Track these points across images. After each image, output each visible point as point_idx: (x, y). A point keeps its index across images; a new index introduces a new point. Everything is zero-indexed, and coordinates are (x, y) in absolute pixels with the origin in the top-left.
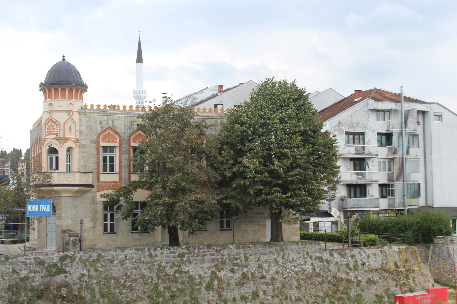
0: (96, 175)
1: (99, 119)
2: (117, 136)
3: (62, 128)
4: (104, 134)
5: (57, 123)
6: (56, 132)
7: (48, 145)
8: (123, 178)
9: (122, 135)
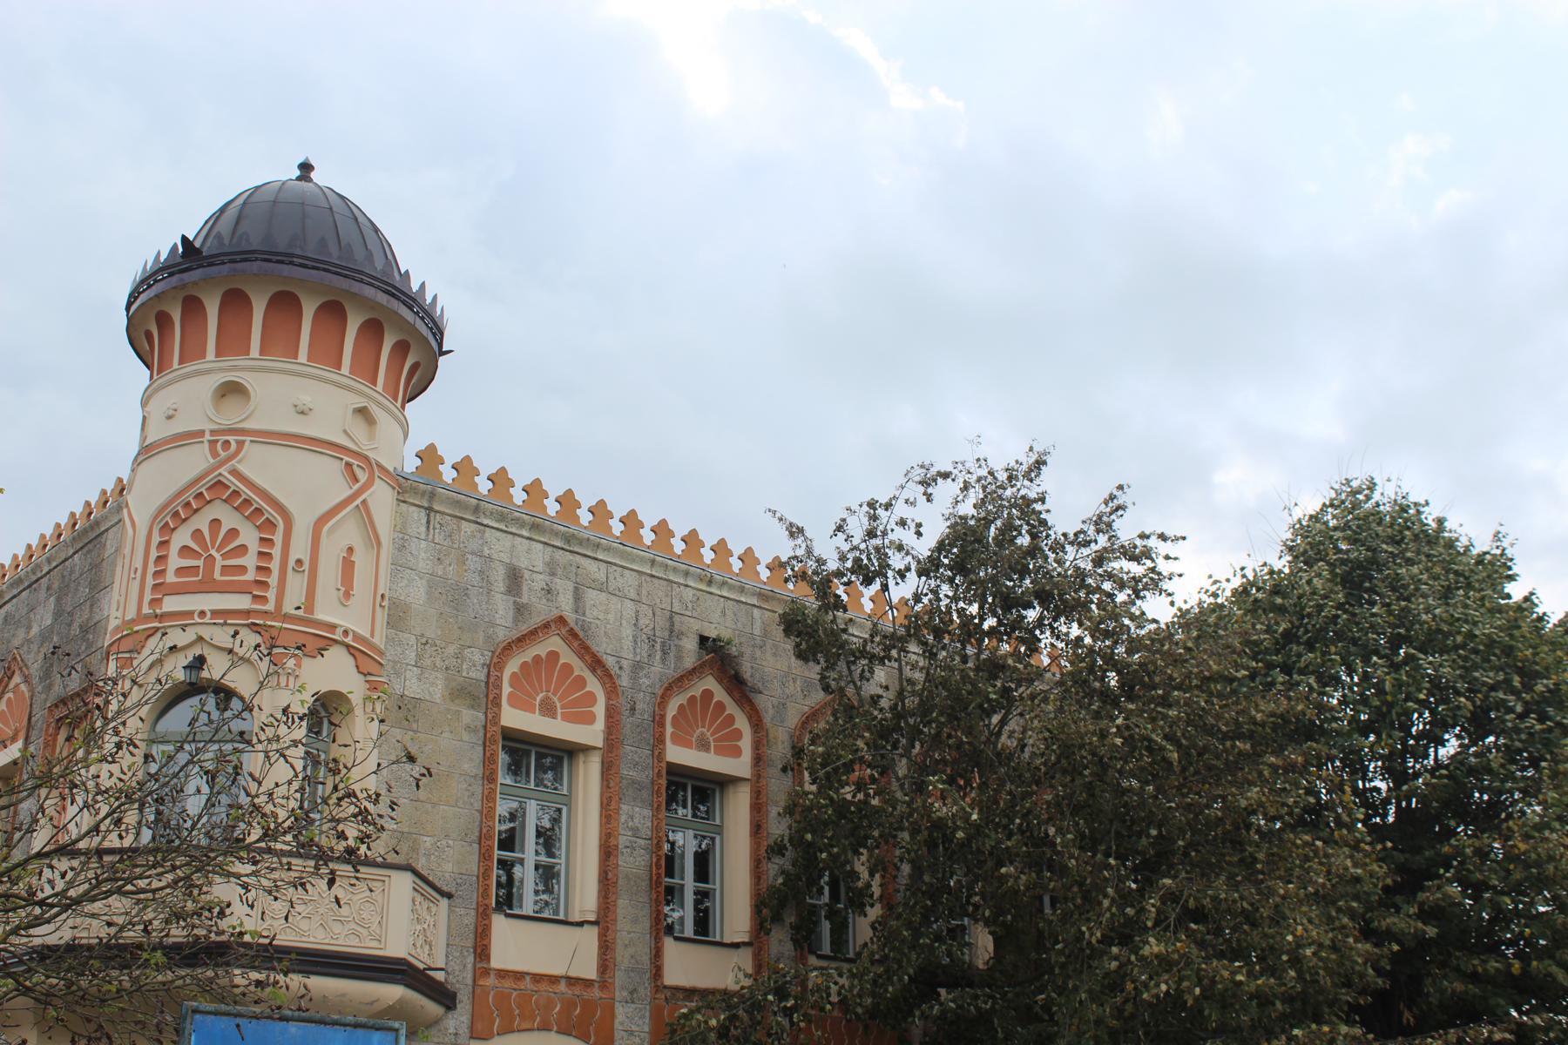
0: (470, 919)
2: (594, 685)
3: (300, 548)
4: (528, 655)
5: (265, 514)
6: (251, 575)
8: (622, 956)
9: (624, 681)
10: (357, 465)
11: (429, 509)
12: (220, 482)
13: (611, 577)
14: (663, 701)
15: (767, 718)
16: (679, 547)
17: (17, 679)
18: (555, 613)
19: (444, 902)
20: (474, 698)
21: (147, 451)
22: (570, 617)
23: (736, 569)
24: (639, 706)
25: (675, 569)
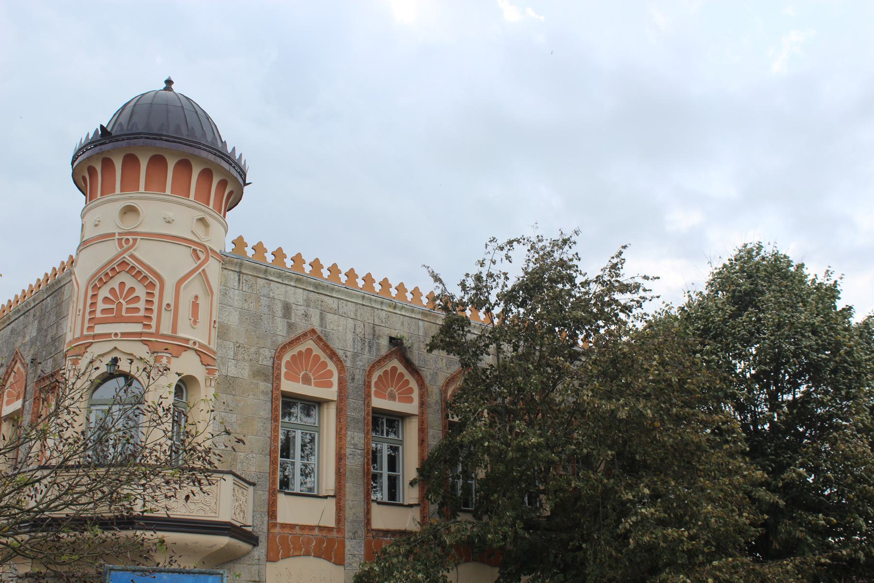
0: (265, 496)
1: (282, 298)
2: (332, 366)
3: (168, 298)
4: (295, 351)
5: (149, 278)
6: (142, 313)
7: (108, 359)
8: (349, 514)
9: (348, 364)
10: (199, 250)
11: (240, 272)
12: (124, 262)
13: (340, 306)
14: (370, 374)
15: (427, 382)
16: (377, 288)
17: (19, 365)
18: (310, 327)
19: (251, 488)
20: (266, 376)
21: (84, 244)
22: (318, 329)
23: (409, 299)
24: (357, 377)
25: (375, 301)
